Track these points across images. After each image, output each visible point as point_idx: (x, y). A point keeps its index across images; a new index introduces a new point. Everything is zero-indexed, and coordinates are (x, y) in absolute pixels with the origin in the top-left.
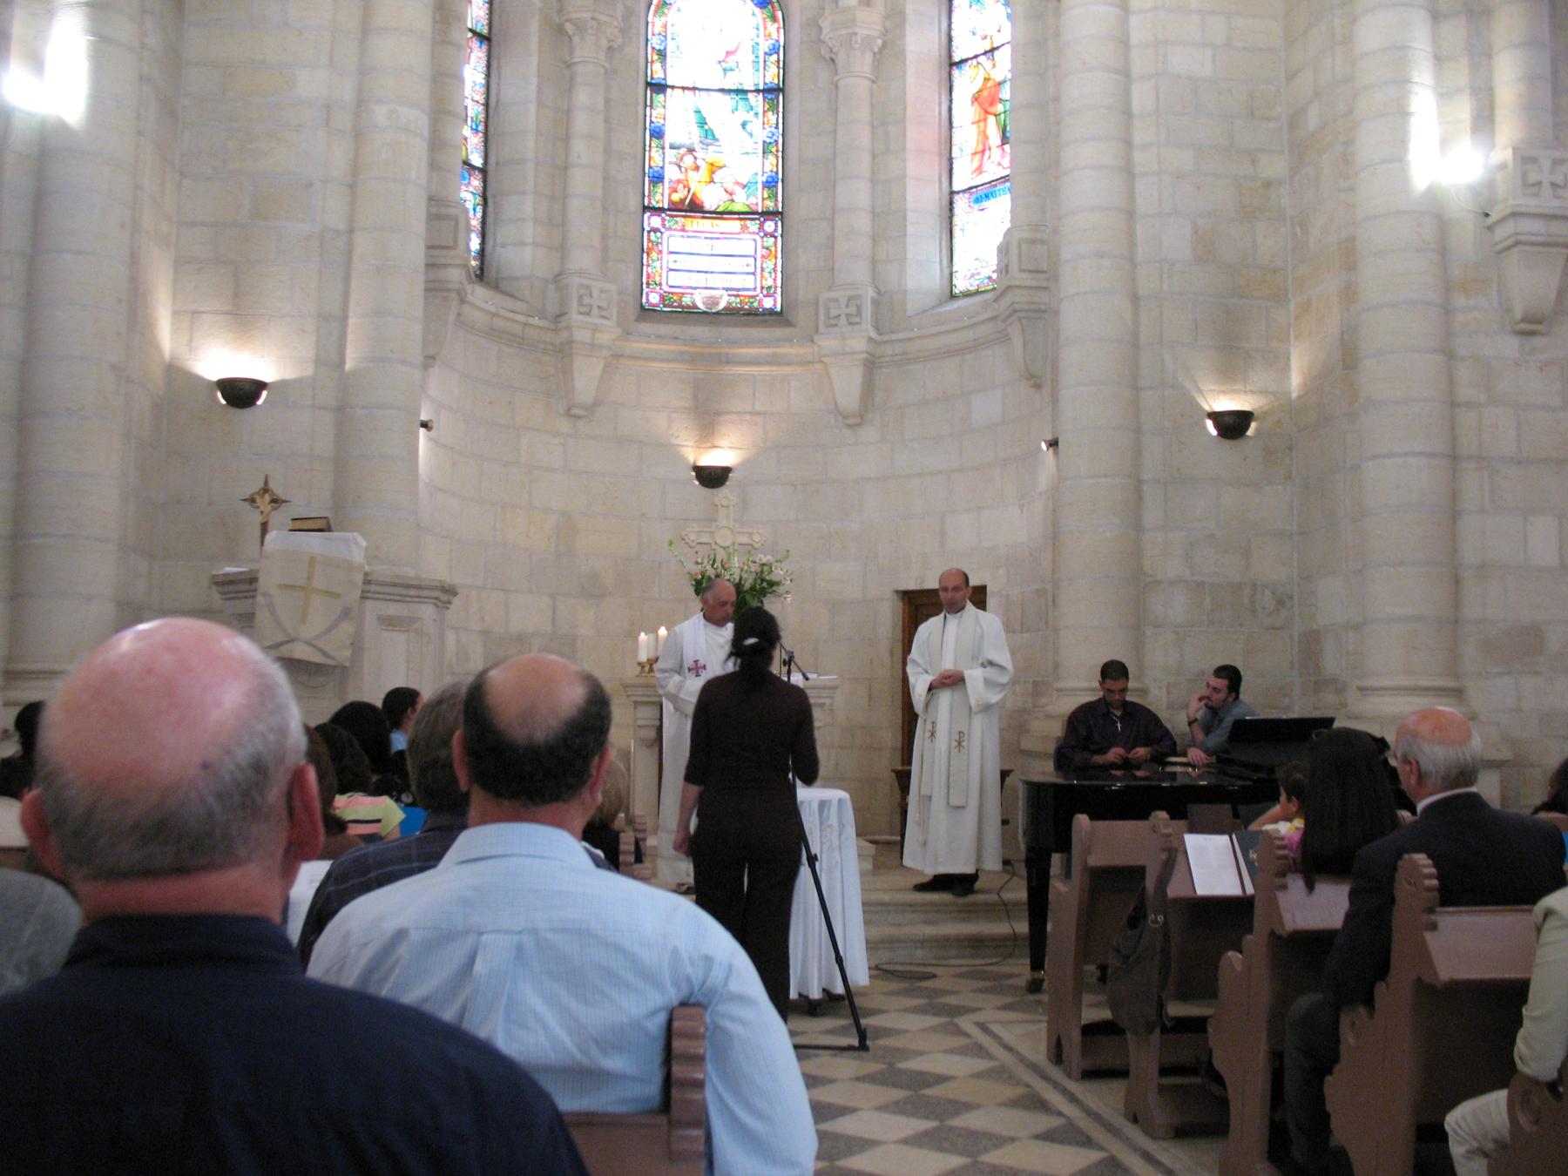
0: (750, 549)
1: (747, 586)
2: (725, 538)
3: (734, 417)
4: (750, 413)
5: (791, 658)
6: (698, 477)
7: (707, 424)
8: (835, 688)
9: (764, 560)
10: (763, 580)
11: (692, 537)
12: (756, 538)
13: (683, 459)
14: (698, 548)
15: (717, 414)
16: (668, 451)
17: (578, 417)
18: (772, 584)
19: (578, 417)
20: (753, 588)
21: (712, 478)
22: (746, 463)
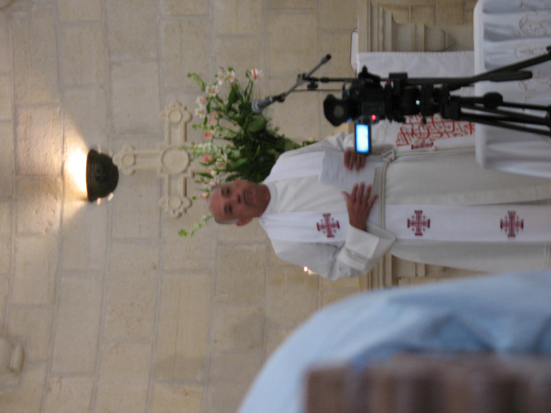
1: (237, 129)
2: (177, 161)
3: (22, 146)
4: (16, 124)
5: (305, 78)
6: (104, 194)
7: (42, 183)
9: (202, 107)
10: (230, 108)
11: (176, 203)
12: (176, 117)
13: (80, 215)
14: (190, 194)
15: (17, 170)
16: (68, 235)
17: (23, 356)
18: (235, 96)
19: (23, 356)
20: (241, 122)
21: (103, 176)
22: (84, 131)
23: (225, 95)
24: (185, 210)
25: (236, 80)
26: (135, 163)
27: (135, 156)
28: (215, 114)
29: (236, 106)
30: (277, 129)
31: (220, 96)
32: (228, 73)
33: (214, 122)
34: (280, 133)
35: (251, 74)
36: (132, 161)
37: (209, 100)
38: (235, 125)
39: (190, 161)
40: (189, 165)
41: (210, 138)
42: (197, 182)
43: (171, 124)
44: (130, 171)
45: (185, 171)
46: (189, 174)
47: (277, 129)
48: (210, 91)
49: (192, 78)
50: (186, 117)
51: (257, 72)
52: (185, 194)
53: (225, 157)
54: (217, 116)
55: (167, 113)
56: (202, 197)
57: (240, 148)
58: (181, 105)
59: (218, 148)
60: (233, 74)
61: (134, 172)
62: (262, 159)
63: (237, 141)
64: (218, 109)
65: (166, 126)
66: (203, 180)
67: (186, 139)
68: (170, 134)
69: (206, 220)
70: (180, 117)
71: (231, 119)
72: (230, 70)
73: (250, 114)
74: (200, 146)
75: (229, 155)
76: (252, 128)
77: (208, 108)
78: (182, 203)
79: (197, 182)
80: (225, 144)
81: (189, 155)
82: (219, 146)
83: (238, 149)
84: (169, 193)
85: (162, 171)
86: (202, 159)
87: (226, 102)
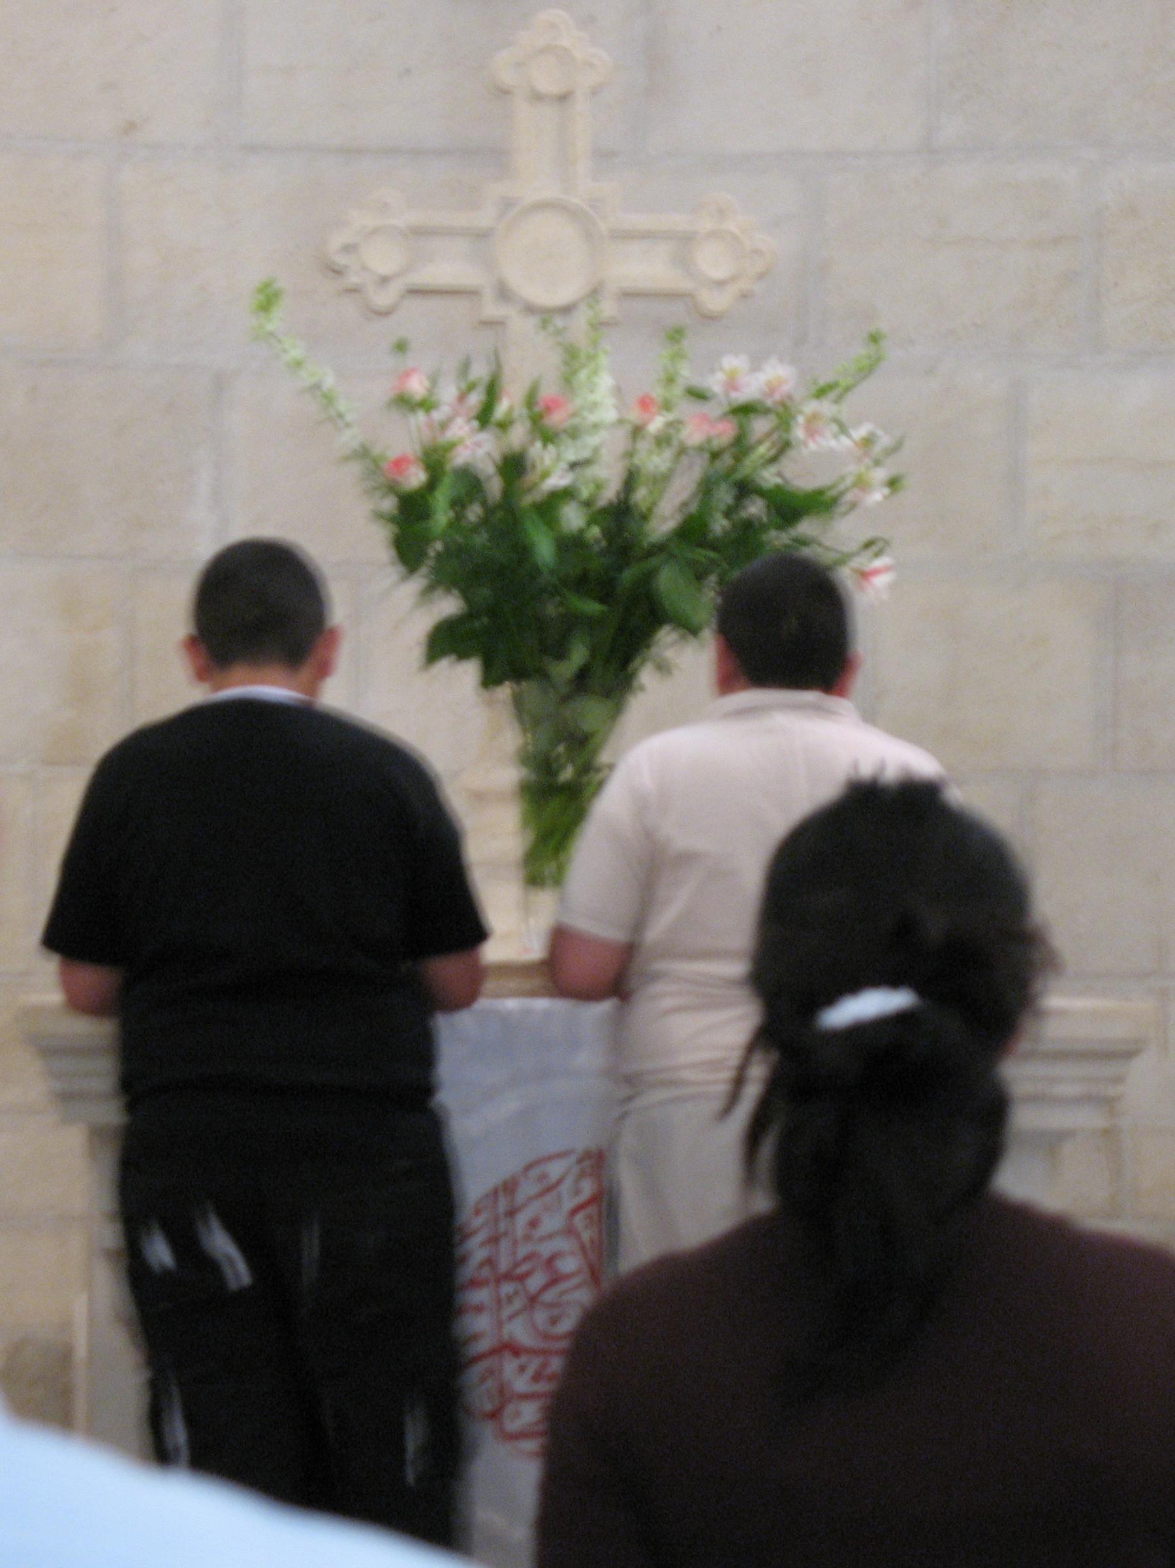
0: (677, 322)
2: (547, 266)
8: (1125, 1053)
9: (751, 388)
10: (745, 489)
11: (383, 258)
12: (713, 262)
14: (415, 319)
20: (692, 531)
23: (798, 474)
24: (354, 290)
25: (854, 506)
26: (537, 97)
27: (564, 98)
28: (724, 433)
29: (755, 508)
30: (663, 668)
31: (792, 453)
32: (880, 475)
33: (693, 435)
34: (646, 676)
35: (877, 555)
36: (547, 84)
37: (784, 414)
38: (685, 504)
39: (545, 315)
40: (530, 309)
41: (635, 416)
42: (465, 367)
43: (685, 241)
44: (508, 77)
45: (504, 293)
46: (491, 309)
47: (663, 668)
48: (814, 418)
49: (861, 351)
50: (715, 301)
51: (881, 581)
52: (417, 292)
53: (557, 480)
54: (716, 444)
55: (731, 226)
56: (407, 374)
57: (595, 531)
58: (761, 276)
59: (596, 450)
60: (877, 496)
61: (504, 92)
62: (551, 609)
63: (620, 516)
64: (741, 445)
65: (679, 221)
66: (472, 387)
67: (628, 295)
68: (647, 235)
69: (316, 387)
70: (719, 273)
71: (706, 488)
72: (893, 483)
73: (725, 566)
74: (605, 381)
75: (567, 494)
76: (669, 581)
77: (745, 411)
78: (385, 280)
79: (465, 367)
80: (607, 478)
81: (567, 310)
82: (604, 451)
83: (591, 521)
84: (419, 232)
85: (507, 204)
86: (548, 391)
87: (769, 478)
